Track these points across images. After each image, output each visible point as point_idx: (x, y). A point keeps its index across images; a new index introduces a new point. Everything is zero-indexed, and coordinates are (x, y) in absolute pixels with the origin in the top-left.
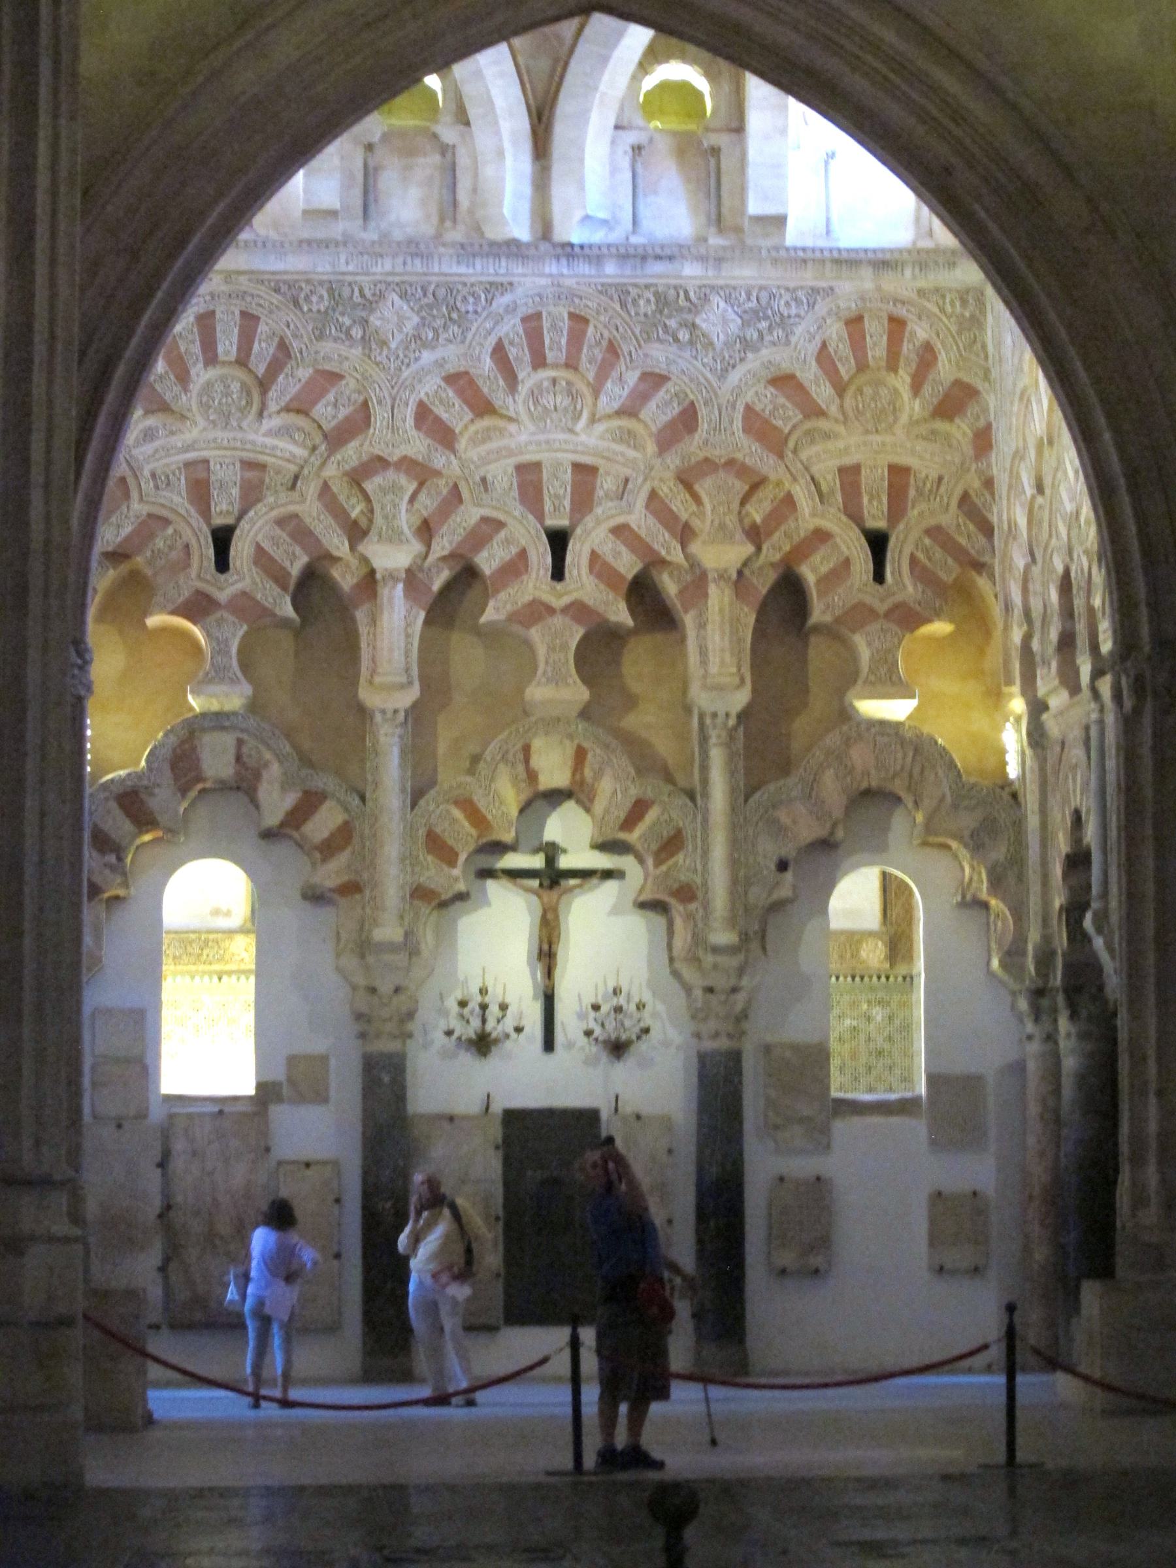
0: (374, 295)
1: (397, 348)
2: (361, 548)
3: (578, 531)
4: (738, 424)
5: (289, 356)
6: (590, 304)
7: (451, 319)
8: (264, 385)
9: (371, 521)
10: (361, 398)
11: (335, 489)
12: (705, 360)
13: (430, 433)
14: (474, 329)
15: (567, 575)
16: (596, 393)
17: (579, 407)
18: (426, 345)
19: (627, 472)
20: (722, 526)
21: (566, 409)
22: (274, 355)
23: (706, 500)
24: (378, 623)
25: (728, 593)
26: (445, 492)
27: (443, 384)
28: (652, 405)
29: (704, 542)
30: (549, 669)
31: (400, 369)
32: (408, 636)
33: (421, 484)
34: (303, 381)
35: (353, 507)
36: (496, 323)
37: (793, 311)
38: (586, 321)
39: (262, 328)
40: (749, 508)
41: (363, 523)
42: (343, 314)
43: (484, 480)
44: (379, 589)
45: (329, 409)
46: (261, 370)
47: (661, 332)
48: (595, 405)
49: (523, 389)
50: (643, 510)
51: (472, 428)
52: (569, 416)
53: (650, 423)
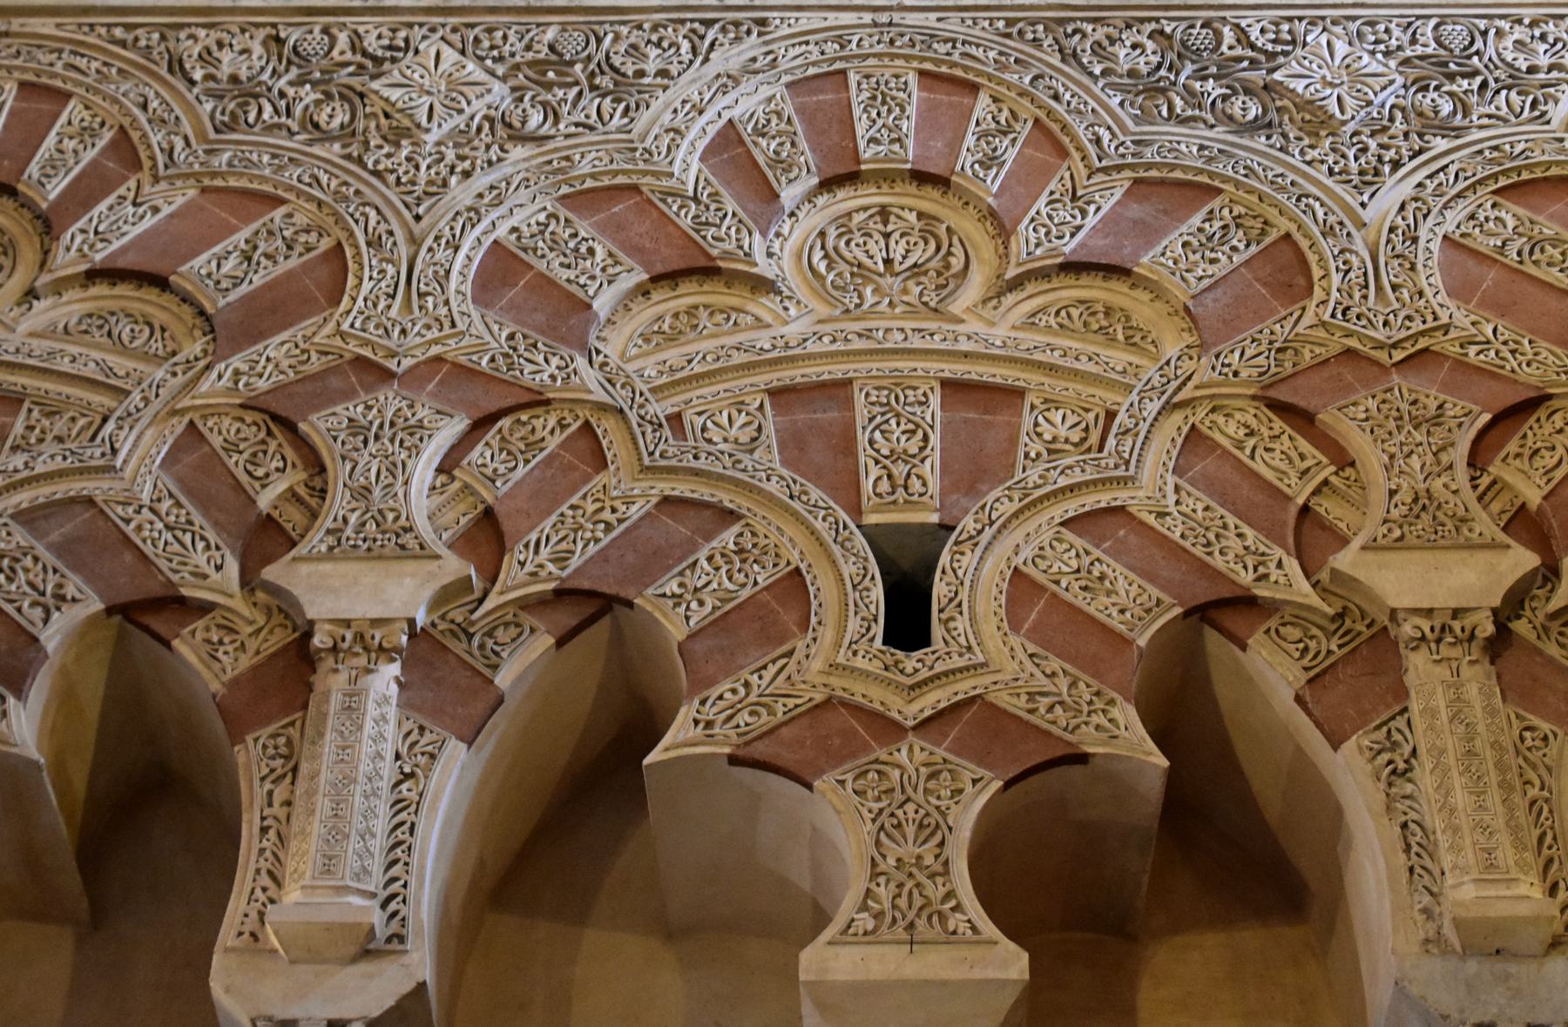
0: (390, 48)
1: (438, 144)
2: (271, 573)
3: (968, 524)
4: (1431, 278)
5: (138, 166)
6: (979, 53)
7: (593, 88)
8: (48, 226)
9: (314, 515)
10: (326, 244)
11: (217, 441)
12: (1312, 154)
13: (515, 310)
14: (655, 105)
15: (937, 631)
16: (1003, 230)
17: (957, 263)
18: (520, 137)
19: (1111, 397)
20: (1422, 503)
21: (917, 270)
22: (94, 163)
23: (1359, 442)
24: (304, 768)
25: (1477, 680)
26: (553, 443)
27: (563, 213)
28: (1173, 242)
29: (1371, 547)
30: (884, 892)
31: (445, 184)
32: (399, 804)
33: (481, 424)
34: (166, 210)
35: (264, 482)
36: (724, 90)
37: (1544, 61)
38: (974, 88)
39: (73, 111)
40: (1496, 469)
41: (292, 517)
42: (298, 82)
43: (676, 420)
44: (318, 680)
45: (227, 267)
46: (56, 188)
47: (1178, 102)
48: (1004, 256)
49: (797, 232)
50: (1171, 480)
51: (644, 314)
52: (929, 281)
53: (1173, 285)
